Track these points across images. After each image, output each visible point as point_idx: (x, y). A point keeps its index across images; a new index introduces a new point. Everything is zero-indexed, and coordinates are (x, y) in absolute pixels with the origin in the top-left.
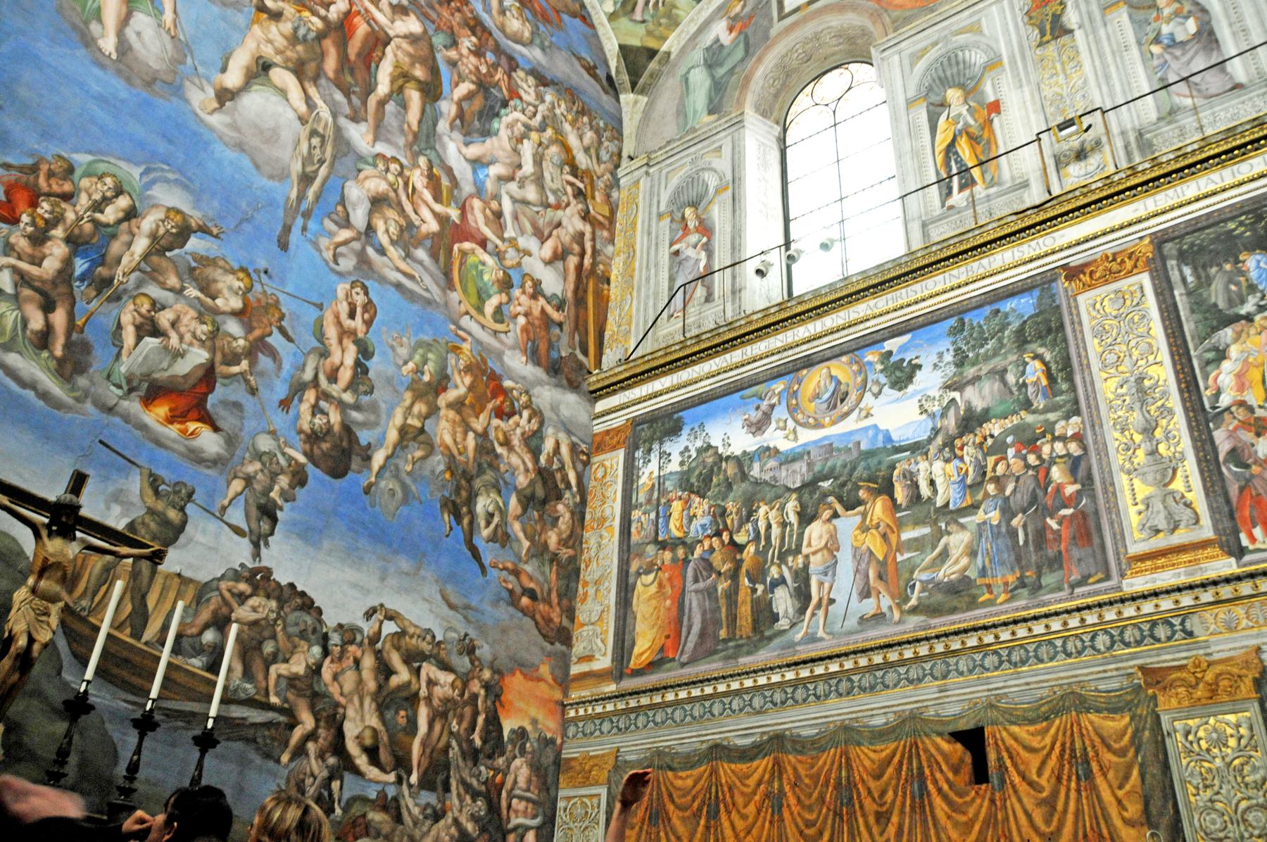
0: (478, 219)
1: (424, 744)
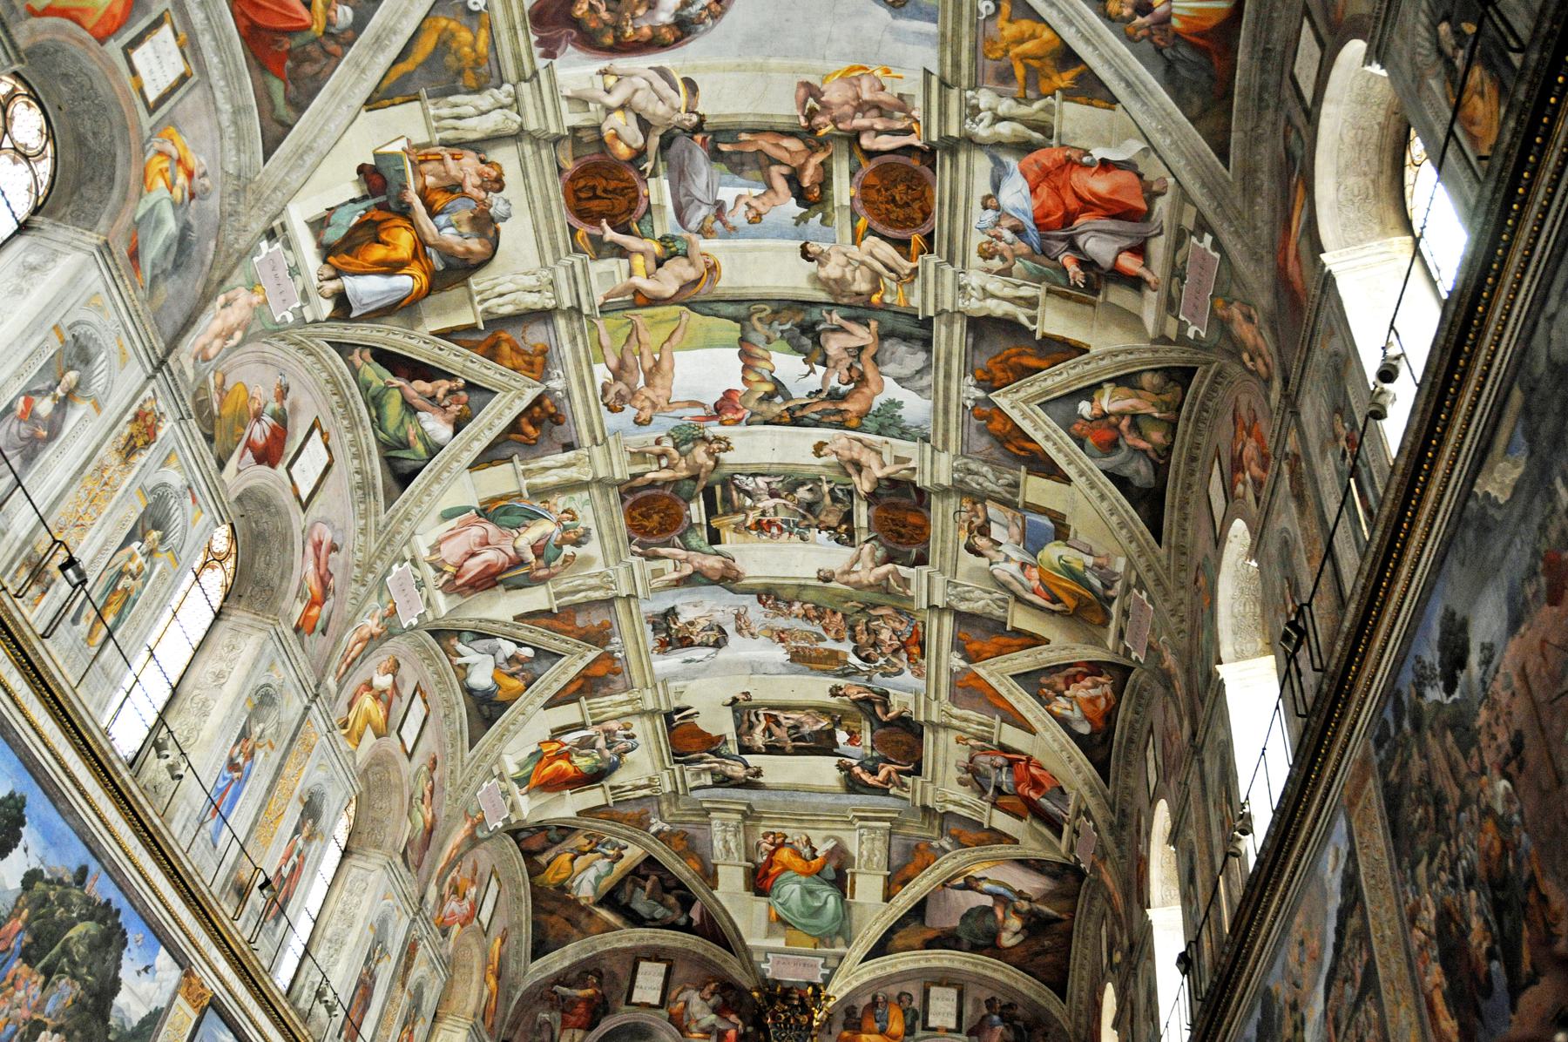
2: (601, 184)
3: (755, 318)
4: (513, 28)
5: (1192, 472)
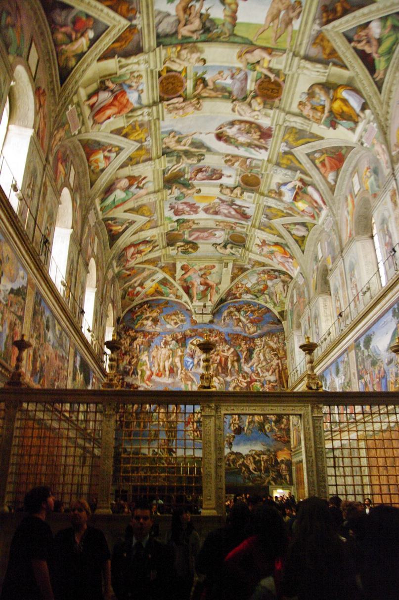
0: (254, 377)
1: (264, 467)
2: (269, 92)
3: (227, 35)
4: (278, 136)
5: (39, 27)
